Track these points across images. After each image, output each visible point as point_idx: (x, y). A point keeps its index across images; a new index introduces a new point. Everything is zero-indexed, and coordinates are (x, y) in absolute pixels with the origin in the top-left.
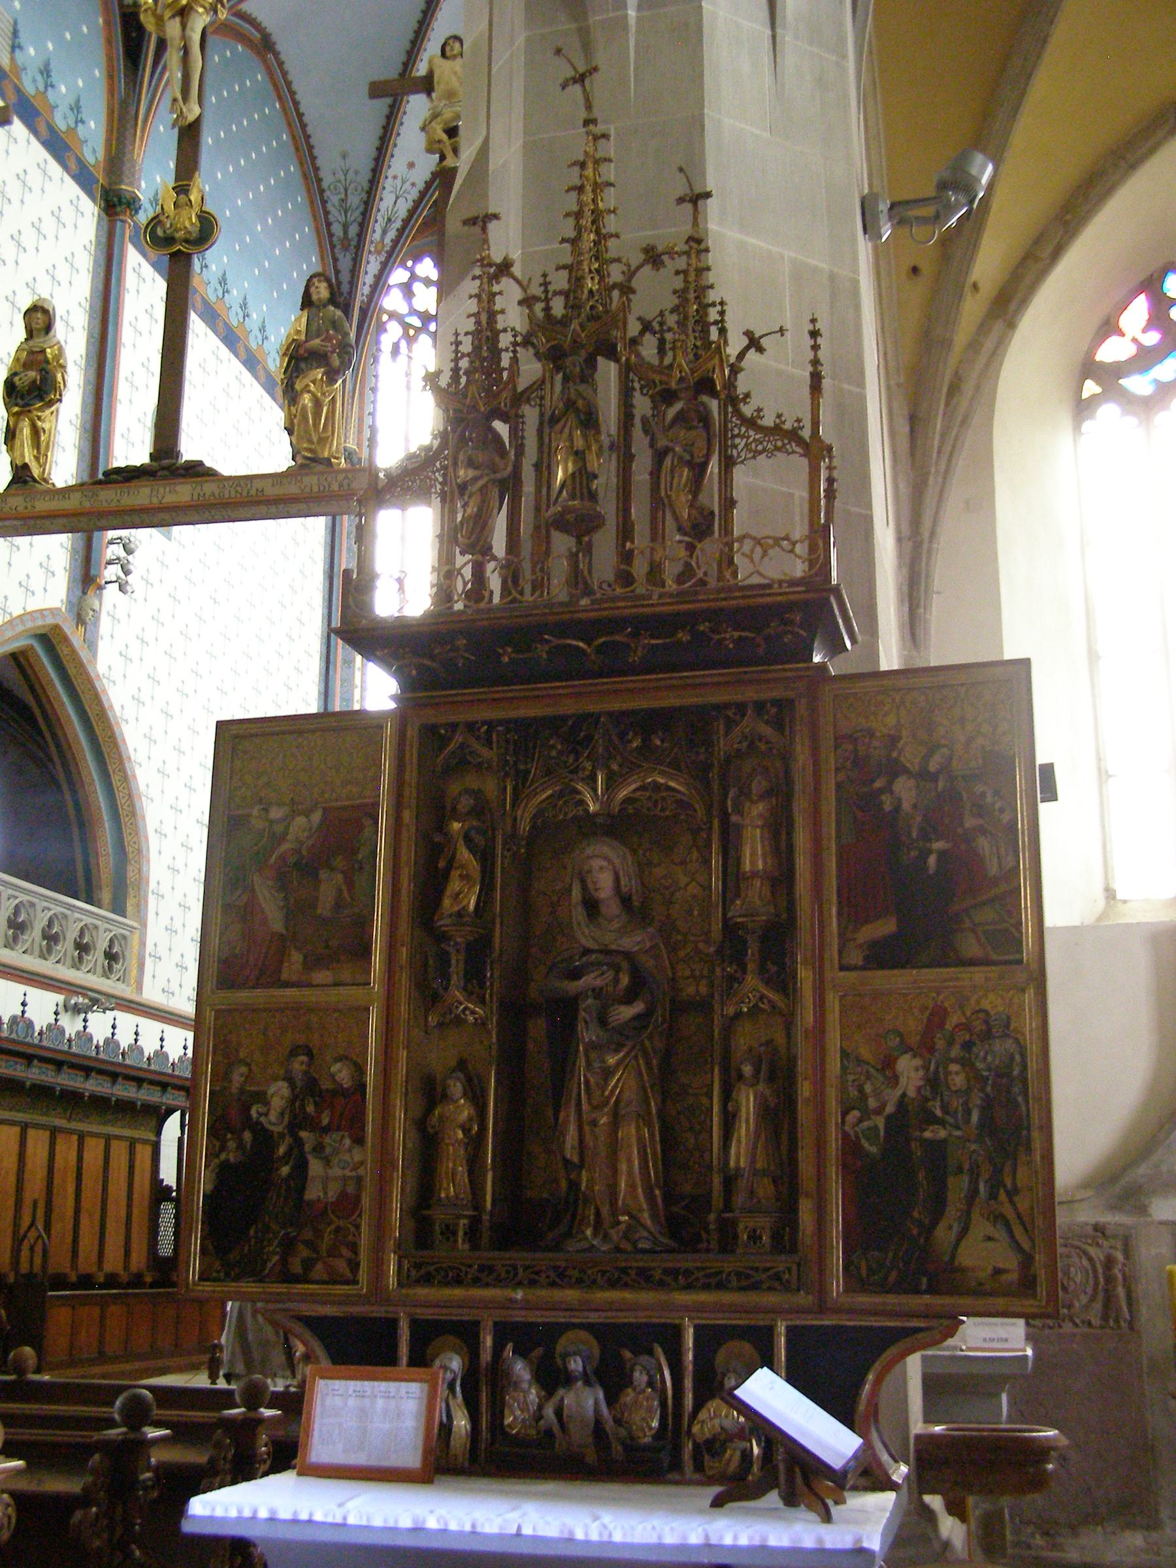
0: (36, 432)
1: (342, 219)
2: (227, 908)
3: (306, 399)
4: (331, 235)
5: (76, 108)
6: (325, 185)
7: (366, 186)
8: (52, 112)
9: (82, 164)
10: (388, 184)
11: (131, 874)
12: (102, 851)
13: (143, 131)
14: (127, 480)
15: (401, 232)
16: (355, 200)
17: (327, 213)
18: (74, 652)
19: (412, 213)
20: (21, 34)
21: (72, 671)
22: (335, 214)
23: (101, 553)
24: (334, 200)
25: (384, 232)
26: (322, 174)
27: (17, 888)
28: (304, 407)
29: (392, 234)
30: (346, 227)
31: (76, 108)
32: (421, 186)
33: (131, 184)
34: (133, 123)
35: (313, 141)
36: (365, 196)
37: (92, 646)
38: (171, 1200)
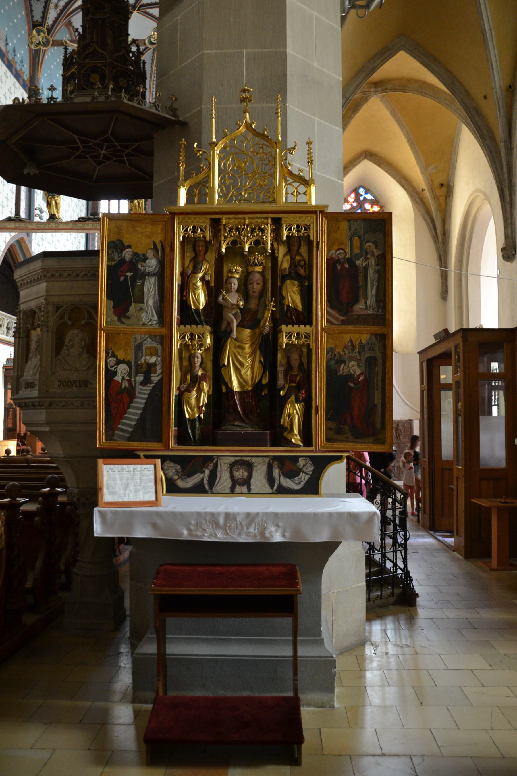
0: (56, 204)
5: (22, 61)
8: (16, 64)
9: (23, 80)
13: (41, 68)
14: (85, 221)
18: (26, 245)
20: (8, 39)
21: (25, 251)
23: (34, 212)
27: (9, 317)
28: (136, 204)
31: (22, 61)
34: (37, 64)
37: (30, 242)
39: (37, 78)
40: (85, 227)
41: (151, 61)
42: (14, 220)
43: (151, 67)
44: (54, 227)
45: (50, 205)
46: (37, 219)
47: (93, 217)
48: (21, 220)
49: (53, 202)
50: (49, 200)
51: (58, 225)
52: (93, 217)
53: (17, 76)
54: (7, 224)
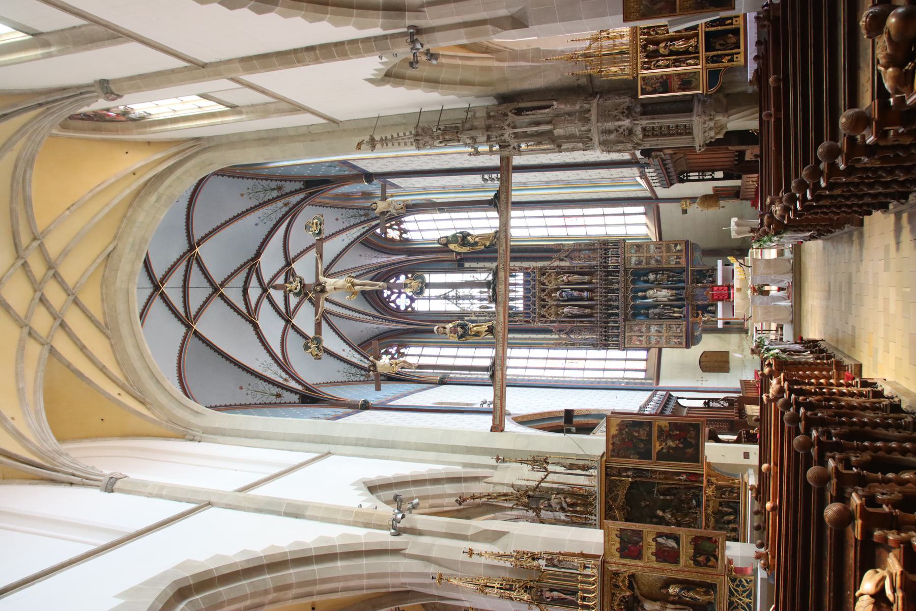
1: (359, 376)
2: (660, 14)
3: (477, 239)
4: (364, 381)
5: (335, 412)
6: (347, 380)
7: (349, 366)
10: (349, 358)
11: (595, 413)
12: (586, 422)
14: (496, 293)
15: (365, 357)
16: (353, 370)
17: (356, 381)
19: (359, 353)
21: (526, 419)
22: (357, 378)
23: (486, 408)
24: (352, 378)
25: (365, 363)
26: (343, 381)
29: (366, 360)
30: (362, 375)
32: (350, 349)
33: (359, 401)
35: (333, 381)
36: (352, 367)
38: (708, 402)
39: (351, 401)
40: (502, 292)
41: (338, 318)
42: (493, 371)
43: (343, 318)
44: (502, 326)
45: (478, 332)
46: (492, 406)
47: (492, 286)
48: (494, 364)
49: (475, 328)
50: (473, 333)
51: (499, 323)
52: (492, 286)
53: (349, 414)
54: (497, 379)
